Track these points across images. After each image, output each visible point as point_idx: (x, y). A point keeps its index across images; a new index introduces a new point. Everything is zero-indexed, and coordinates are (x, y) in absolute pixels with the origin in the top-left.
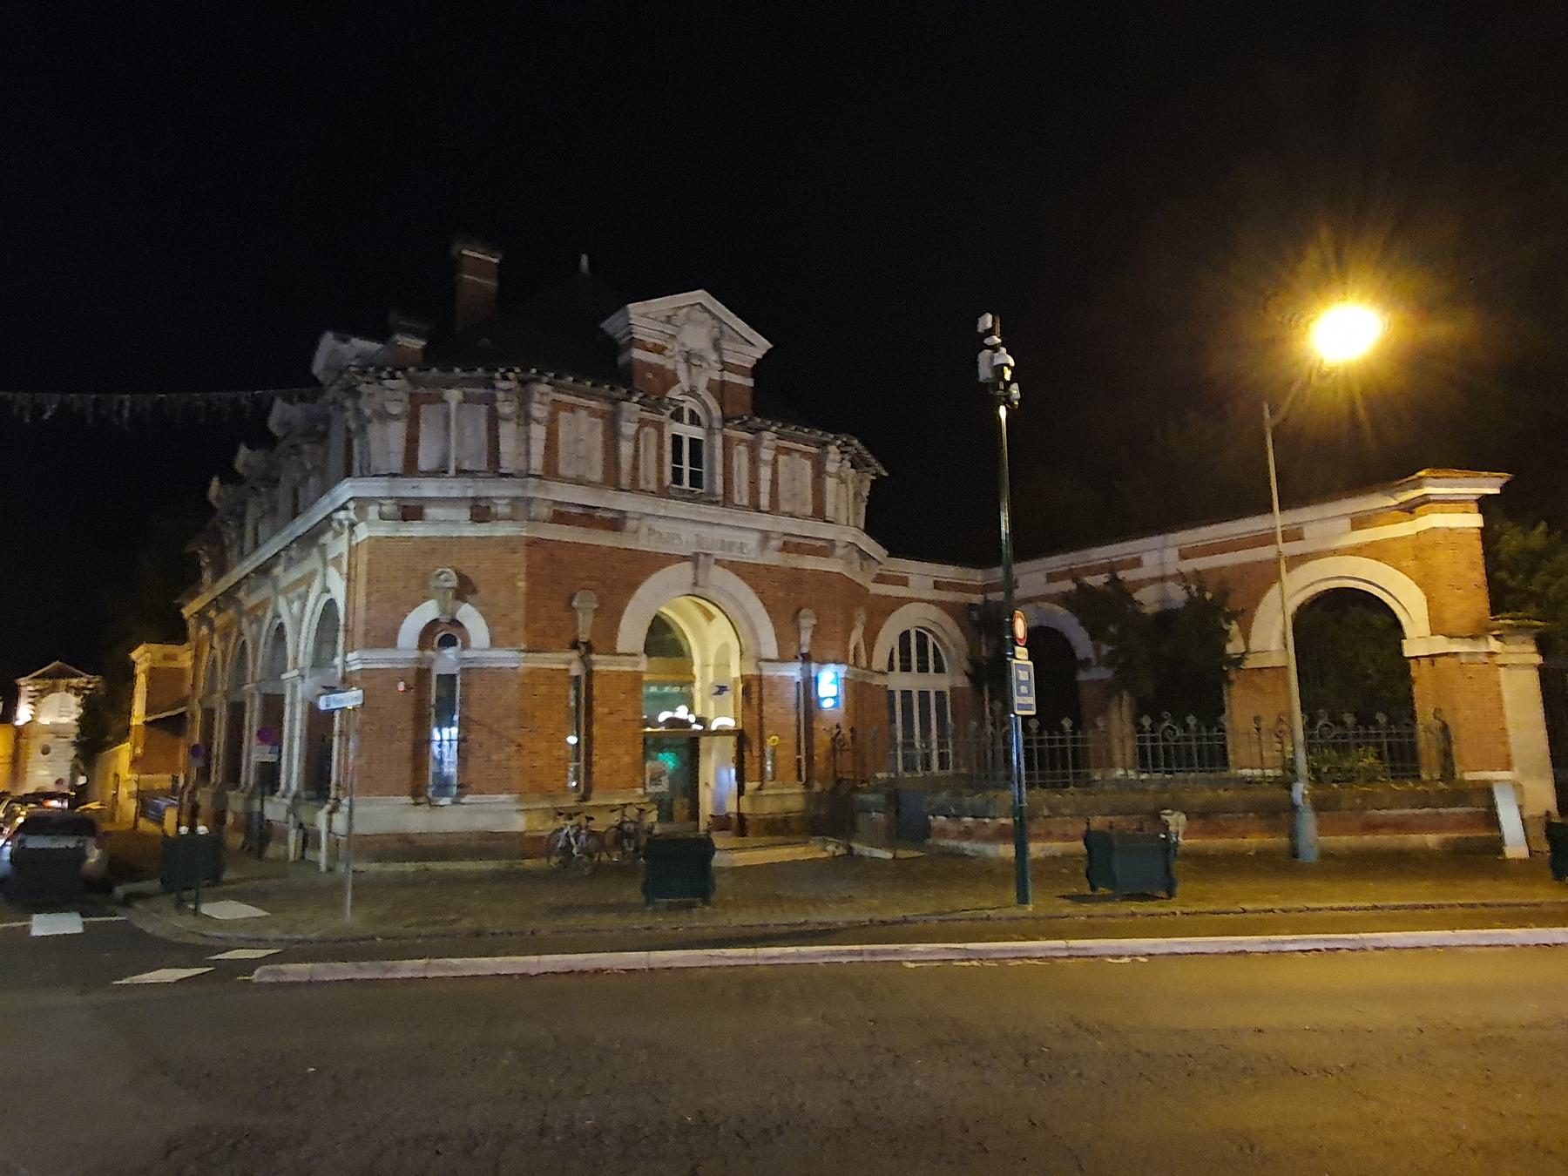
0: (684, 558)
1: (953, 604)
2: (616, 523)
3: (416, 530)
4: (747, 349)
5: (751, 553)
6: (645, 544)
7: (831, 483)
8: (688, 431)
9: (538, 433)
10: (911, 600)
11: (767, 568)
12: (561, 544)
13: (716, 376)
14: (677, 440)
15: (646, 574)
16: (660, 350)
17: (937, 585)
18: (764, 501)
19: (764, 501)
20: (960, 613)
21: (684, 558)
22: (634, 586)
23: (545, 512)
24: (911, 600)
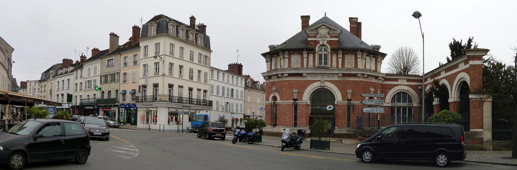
0: (318, 81)
1: (413, 85)
2: (301, 75)
3: (271, 81)
4: (335, 32)
5: (336, 78)
6: (309, 78)
7: (359, 60)
8: (323, 53)
9: (287, 60)
10: (399, 85)
11: (340, 81)
12: (291, 81)
13: (329, 39)
14: (320, 56)
15: (309, 85)
16: (314, 37)
17: (408, 81)
18: (340, 66)
19: (340, 66)
20: (414, 87)
21: (318, 81)
22: (307, 87)
23: (287, 75)
24: (399, 85)
